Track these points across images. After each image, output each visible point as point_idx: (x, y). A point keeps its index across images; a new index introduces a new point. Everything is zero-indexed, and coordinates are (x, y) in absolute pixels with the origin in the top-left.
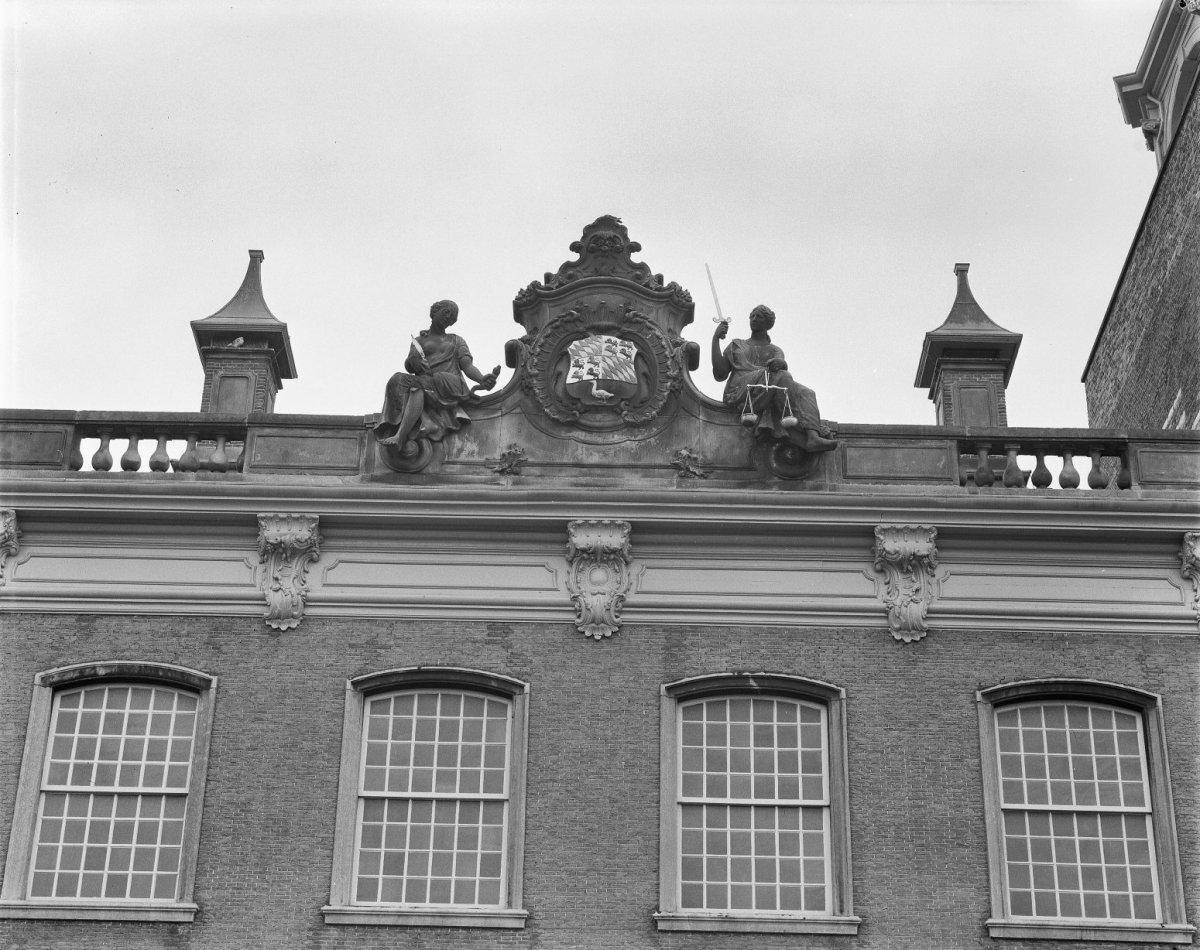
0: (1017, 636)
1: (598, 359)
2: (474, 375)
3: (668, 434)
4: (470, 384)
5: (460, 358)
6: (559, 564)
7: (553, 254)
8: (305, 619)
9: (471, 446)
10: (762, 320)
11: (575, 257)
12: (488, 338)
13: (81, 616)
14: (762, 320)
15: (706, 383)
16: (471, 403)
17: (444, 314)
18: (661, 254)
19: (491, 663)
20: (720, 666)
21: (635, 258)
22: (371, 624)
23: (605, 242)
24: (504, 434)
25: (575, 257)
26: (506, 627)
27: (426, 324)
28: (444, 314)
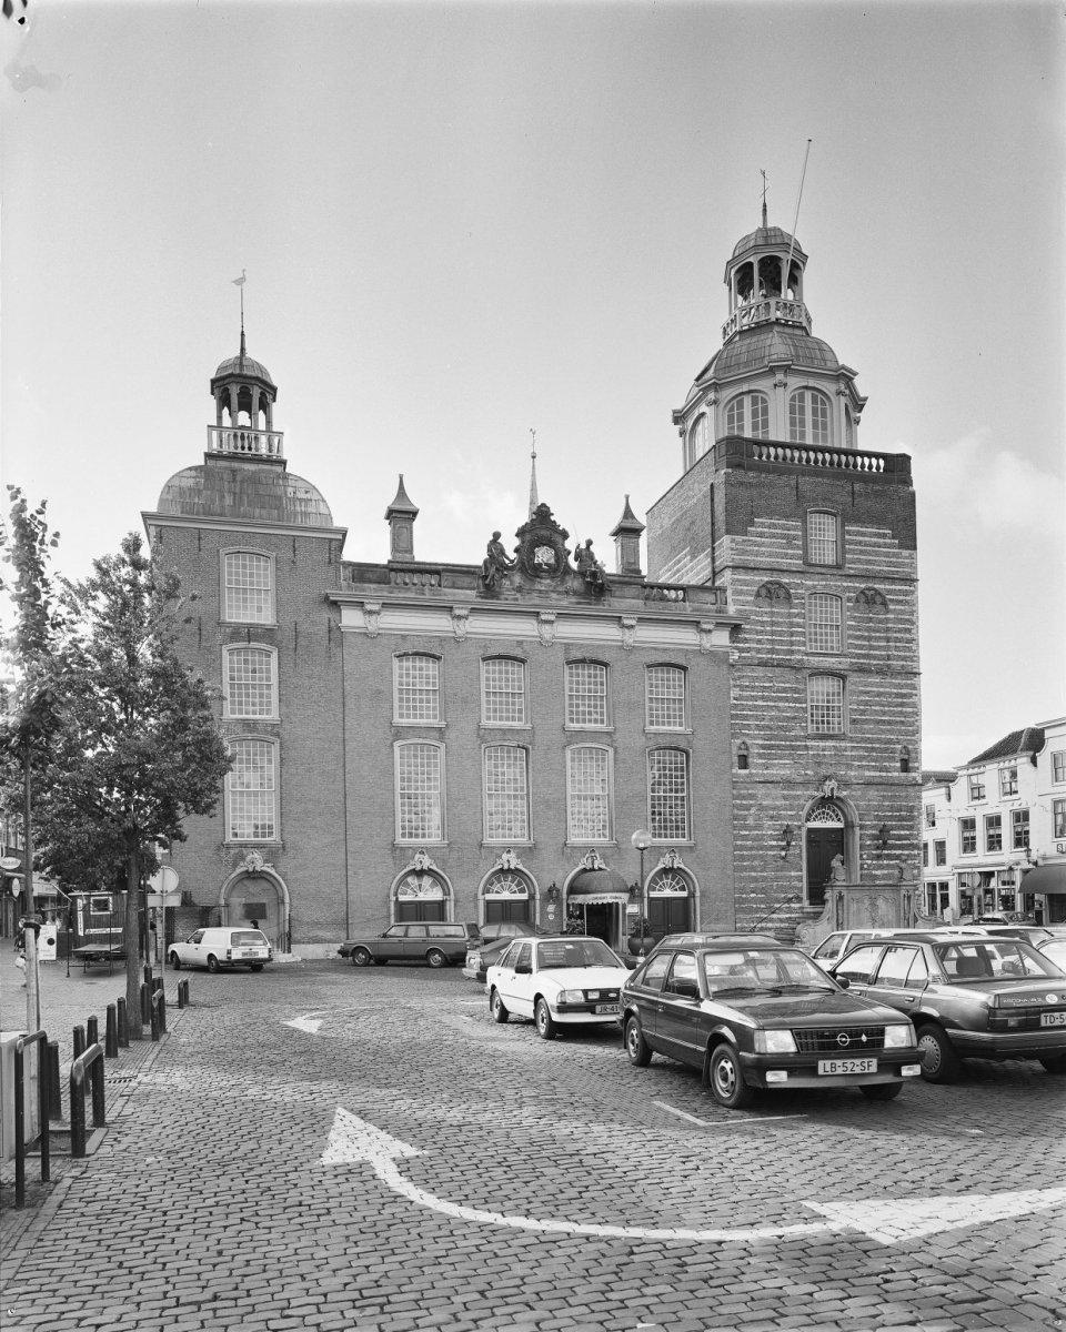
0: (655, 649)
1: (544, 556)
2: (508, 558)
3: (563, 581)
4: (507, 562)
5: (502, 552)
6: (535, 622)
8: (466, 638)
9: (508, 583)
10: (589, 543)
11: (534, 517)
12: (510, 544)
13: (402, 636)
14: (589, 543)
15: (574, 565)
16: (507, 568)
17: (497, 536)
18: (560, 518)
19: (518, 652)
20: (579, 655)
21: (552, 518)
22: (484, 642)
23: (542, 515)
24: (517, 579)
25: (534, 517)
26: (522, 642)
27: (491, 538)
28: (497, 536)
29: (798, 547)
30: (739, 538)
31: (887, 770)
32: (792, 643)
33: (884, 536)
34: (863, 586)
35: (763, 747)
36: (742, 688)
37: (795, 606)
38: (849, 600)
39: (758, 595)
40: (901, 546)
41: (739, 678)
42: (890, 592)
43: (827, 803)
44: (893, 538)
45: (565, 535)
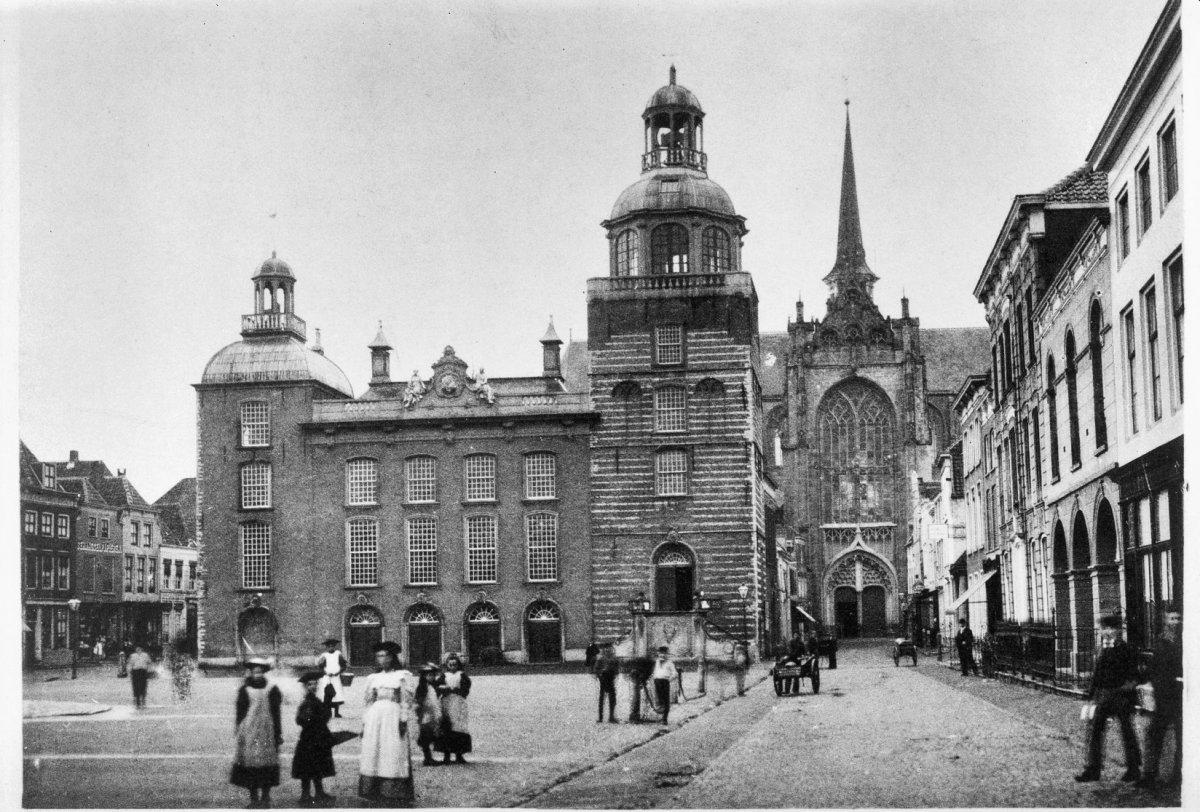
7: (437, 356)
18: (460, 355)
23: (449, 352)
29: (646, 353)
30: (598, 352)
31: (725, 519)
32: (642, 427)
33: (722, 336)
34: (703, 377)
35: (618, 507)
36: (600, 464)
37: (646, 398)
38: (691, 389)
39: (614, 393)
40: (738, 342)
41: (598, 457)
42: (724, 380)
43: (675, 548)
44: (729, 336)
45: (465, 366)
